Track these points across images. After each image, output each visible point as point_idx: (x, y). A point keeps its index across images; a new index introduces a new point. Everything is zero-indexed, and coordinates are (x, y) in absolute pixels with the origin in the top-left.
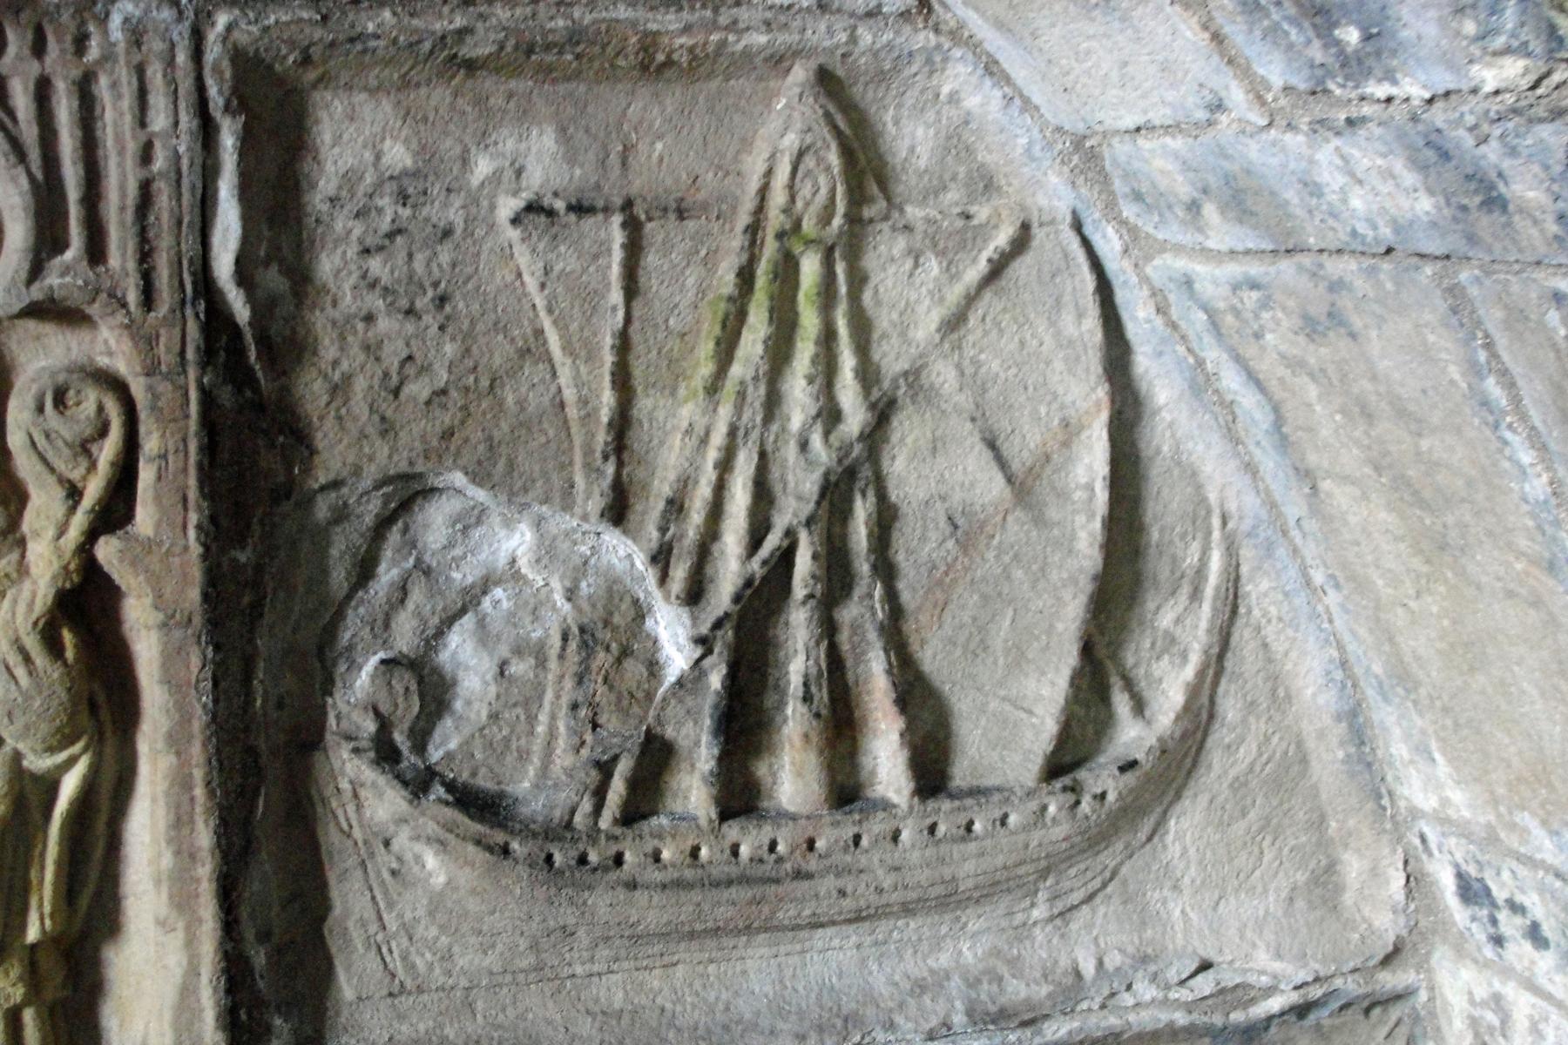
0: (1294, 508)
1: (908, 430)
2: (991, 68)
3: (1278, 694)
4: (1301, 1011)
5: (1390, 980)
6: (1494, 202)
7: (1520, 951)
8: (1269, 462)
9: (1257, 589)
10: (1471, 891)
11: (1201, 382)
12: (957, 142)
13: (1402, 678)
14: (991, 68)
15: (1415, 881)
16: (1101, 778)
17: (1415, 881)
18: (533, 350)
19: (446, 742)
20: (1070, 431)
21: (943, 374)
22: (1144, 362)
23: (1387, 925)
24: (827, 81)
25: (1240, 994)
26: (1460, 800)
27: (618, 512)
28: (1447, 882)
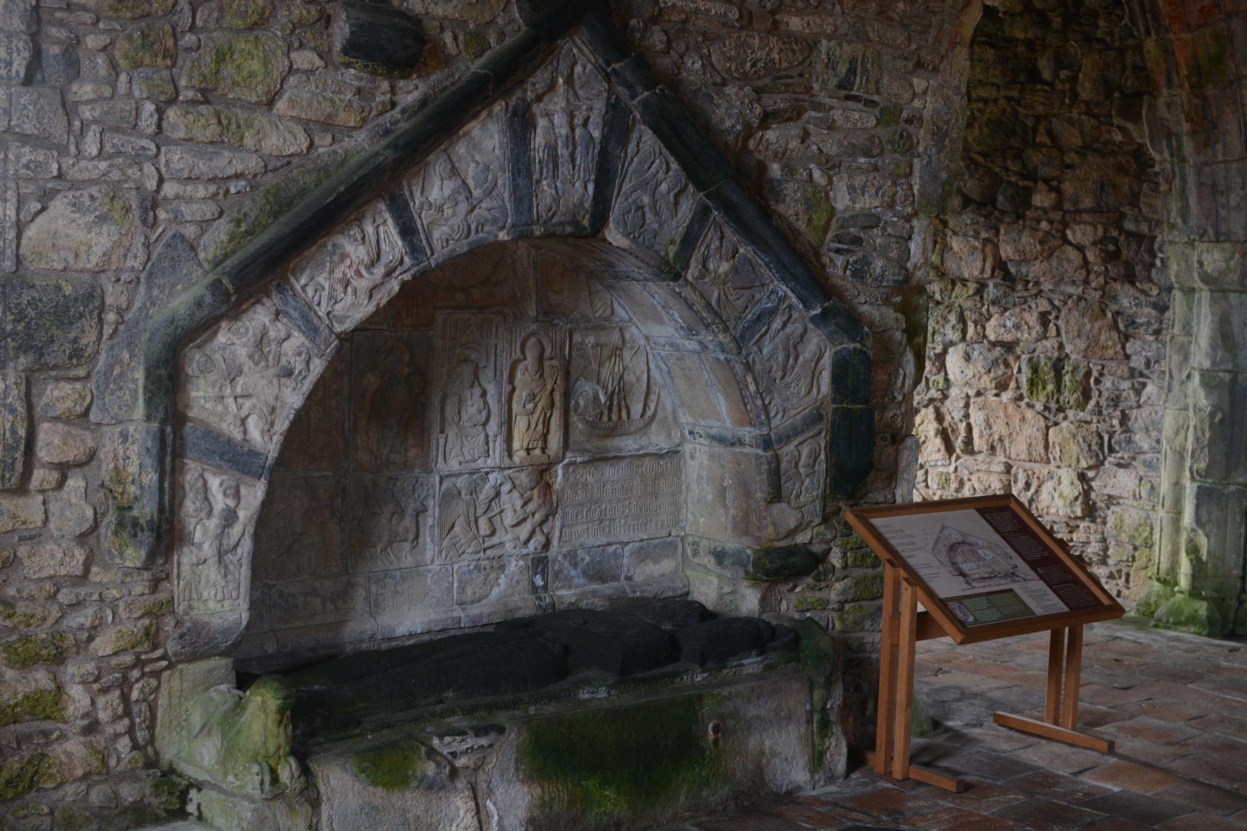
0: (669, 382)
1: (626, 373)
2: (637, 327)
3: (664, 408)
4: (668, 452)
5: (679, 449)
6: (707, 347)
7: (698, 439)
8: (666, 376)
9: (662, 393)
10: (691, 433)
11: (658, 366)
12: (632, 337)
13: (683, 404)
14: (637, 327)
15: (682, 434)
16: (646, 417)
17: (682, 434)
18: (590, 363)
19: (579, 411)
20: (643, 372)
21: (630, 365)
22: (650, 363)
23: (678, 441)
24: (620, 330)
25: (661, 449)
26: (690, 420)
27: (598, 382)
28: (687, 432)
